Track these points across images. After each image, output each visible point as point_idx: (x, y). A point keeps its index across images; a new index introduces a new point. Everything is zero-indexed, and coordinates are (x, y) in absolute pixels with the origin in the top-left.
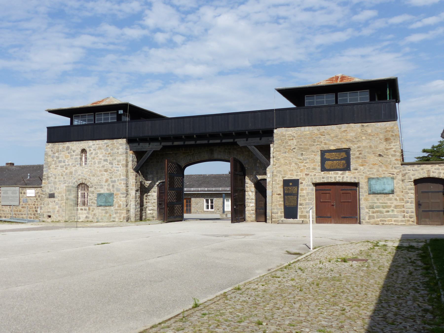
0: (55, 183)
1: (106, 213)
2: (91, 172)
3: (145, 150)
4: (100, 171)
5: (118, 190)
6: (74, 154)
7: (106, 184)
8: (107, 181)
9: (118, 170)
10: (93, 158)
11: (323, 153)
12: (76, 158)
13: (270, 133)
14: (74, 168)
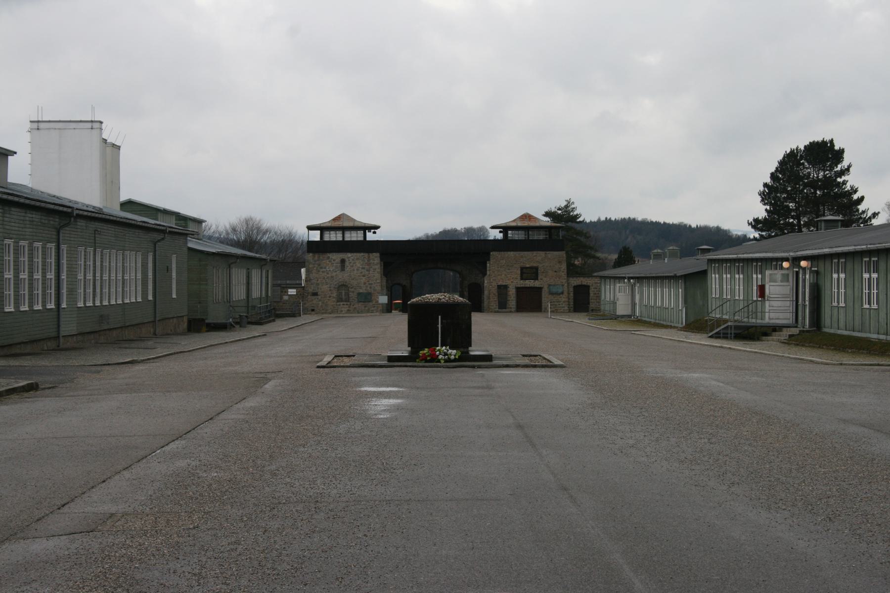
0: (318, 284)
5: (375, 290)
8: (365, 283)
11: (522, 269)
14: (334, 274)
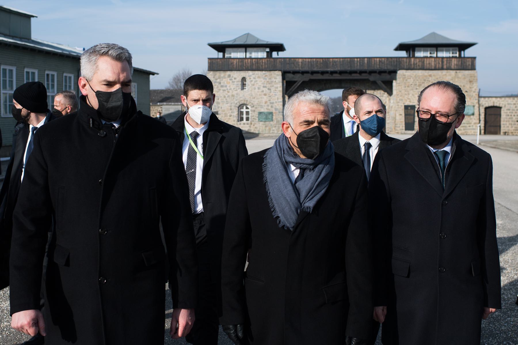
1: (266, 127)
2: (252, 95)
3: (296, 80)
4: (260, 95)
5: (276, 109)
6: (235, 80)
7: (266, 105)
8: (266, 102)
9: (275, 95)
10: (253, 85)
12: (238, 84)
13: (395, 72)
14: (236, 92)
